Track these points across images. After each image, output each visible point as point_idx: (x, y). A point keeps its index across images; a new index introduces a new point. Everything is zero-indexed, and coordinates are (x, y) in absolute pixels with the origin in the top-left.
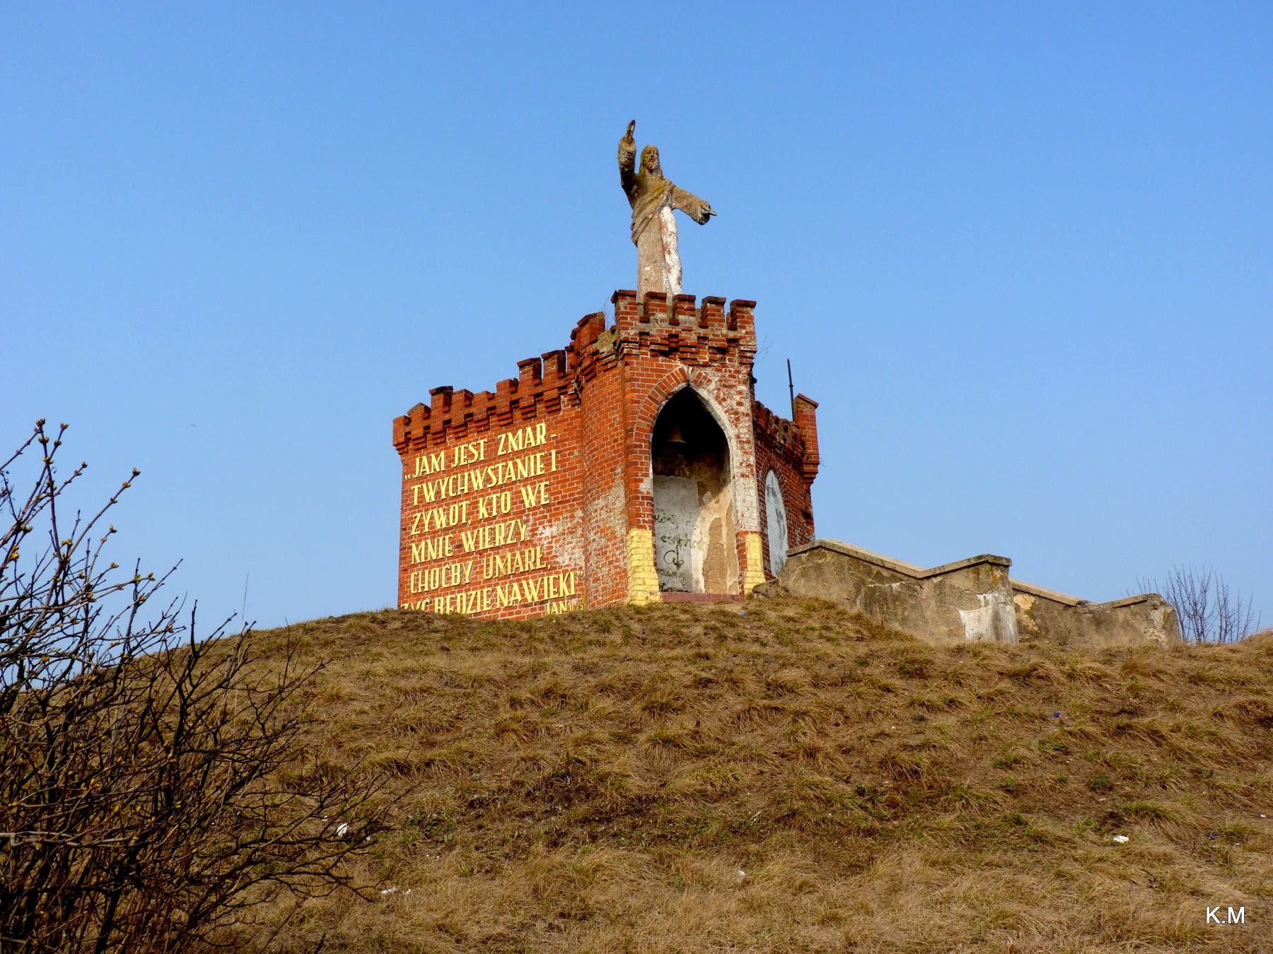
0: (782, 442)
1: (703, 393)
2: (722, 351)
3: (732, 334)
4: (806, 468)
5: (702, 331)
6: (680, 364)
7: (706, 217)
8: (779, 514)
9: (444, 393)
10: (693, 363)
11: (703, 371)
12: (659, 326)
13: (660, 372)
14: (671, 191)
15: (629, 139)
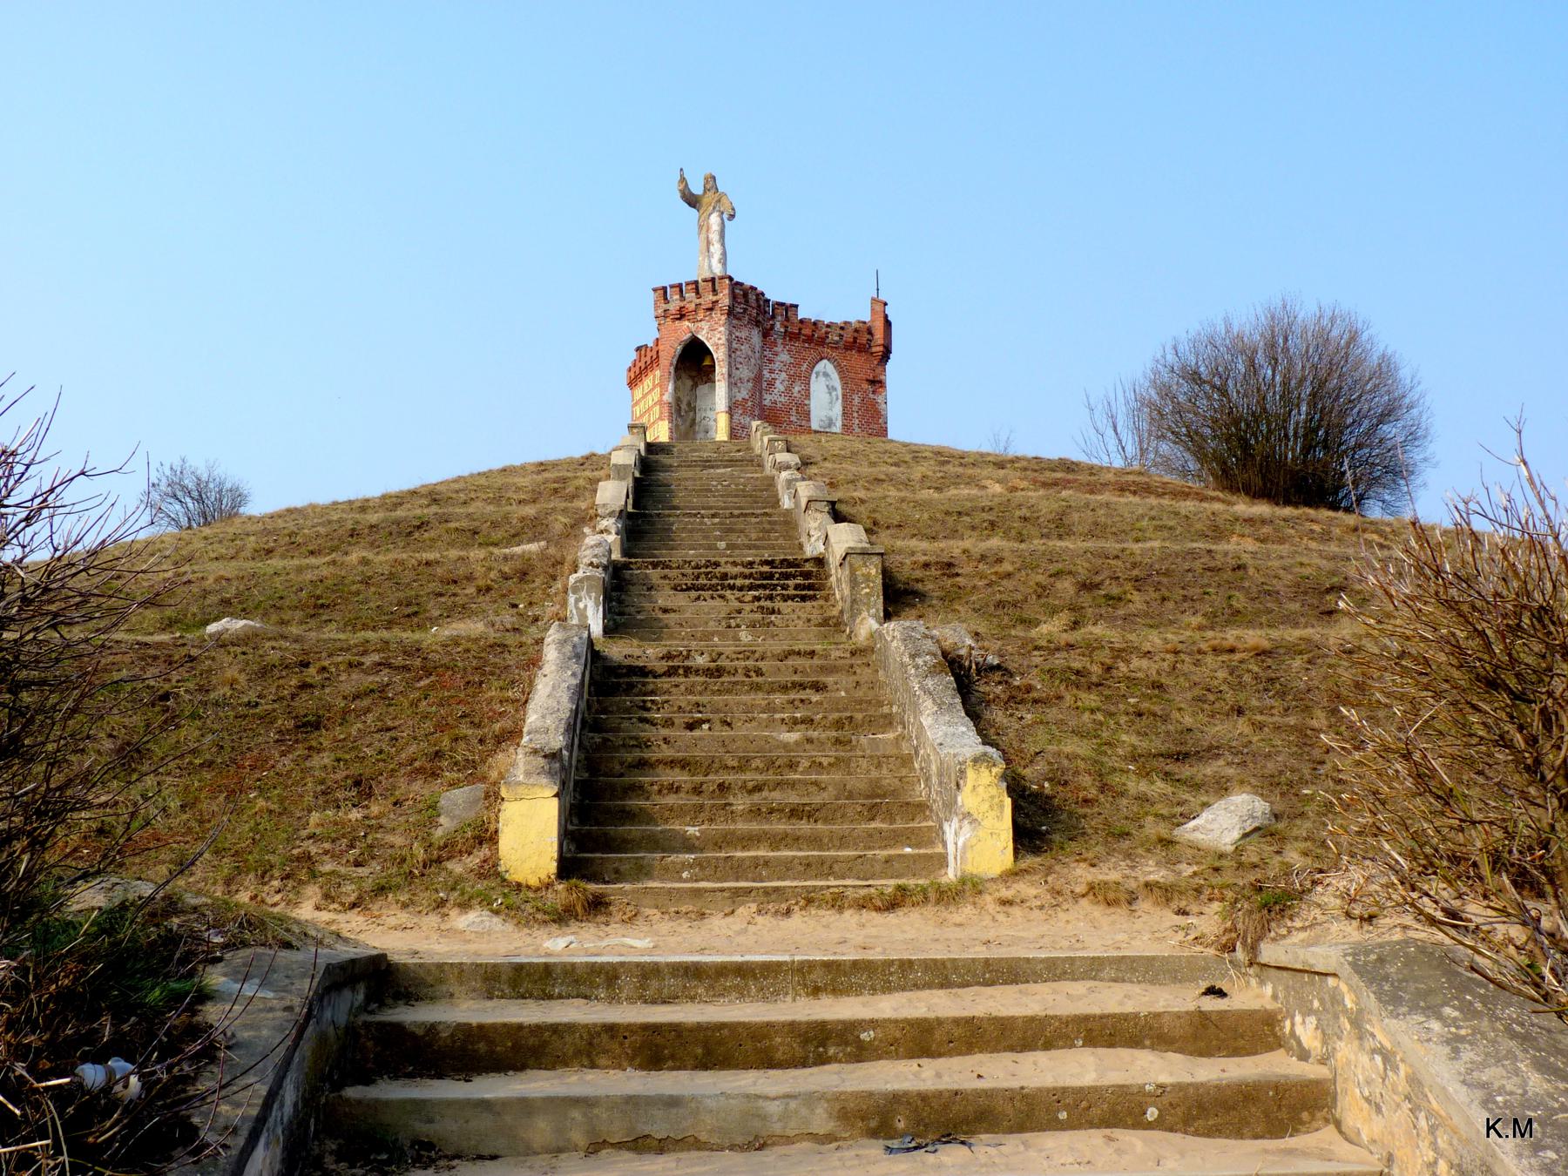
0: (837, 338)
1: (700, 337)
2: (711, 309)
3: (715, 298)
4: (874, 350)
5: (698, 301)
6: (687, 323)
7: (732, 217)
8: (831, 389)
9: (638, 349)
10: (695, 321)
11: (699, 324)
12: (675, 304)
13: (675, 331)
14: (719, 201)
15: (683, 179)
